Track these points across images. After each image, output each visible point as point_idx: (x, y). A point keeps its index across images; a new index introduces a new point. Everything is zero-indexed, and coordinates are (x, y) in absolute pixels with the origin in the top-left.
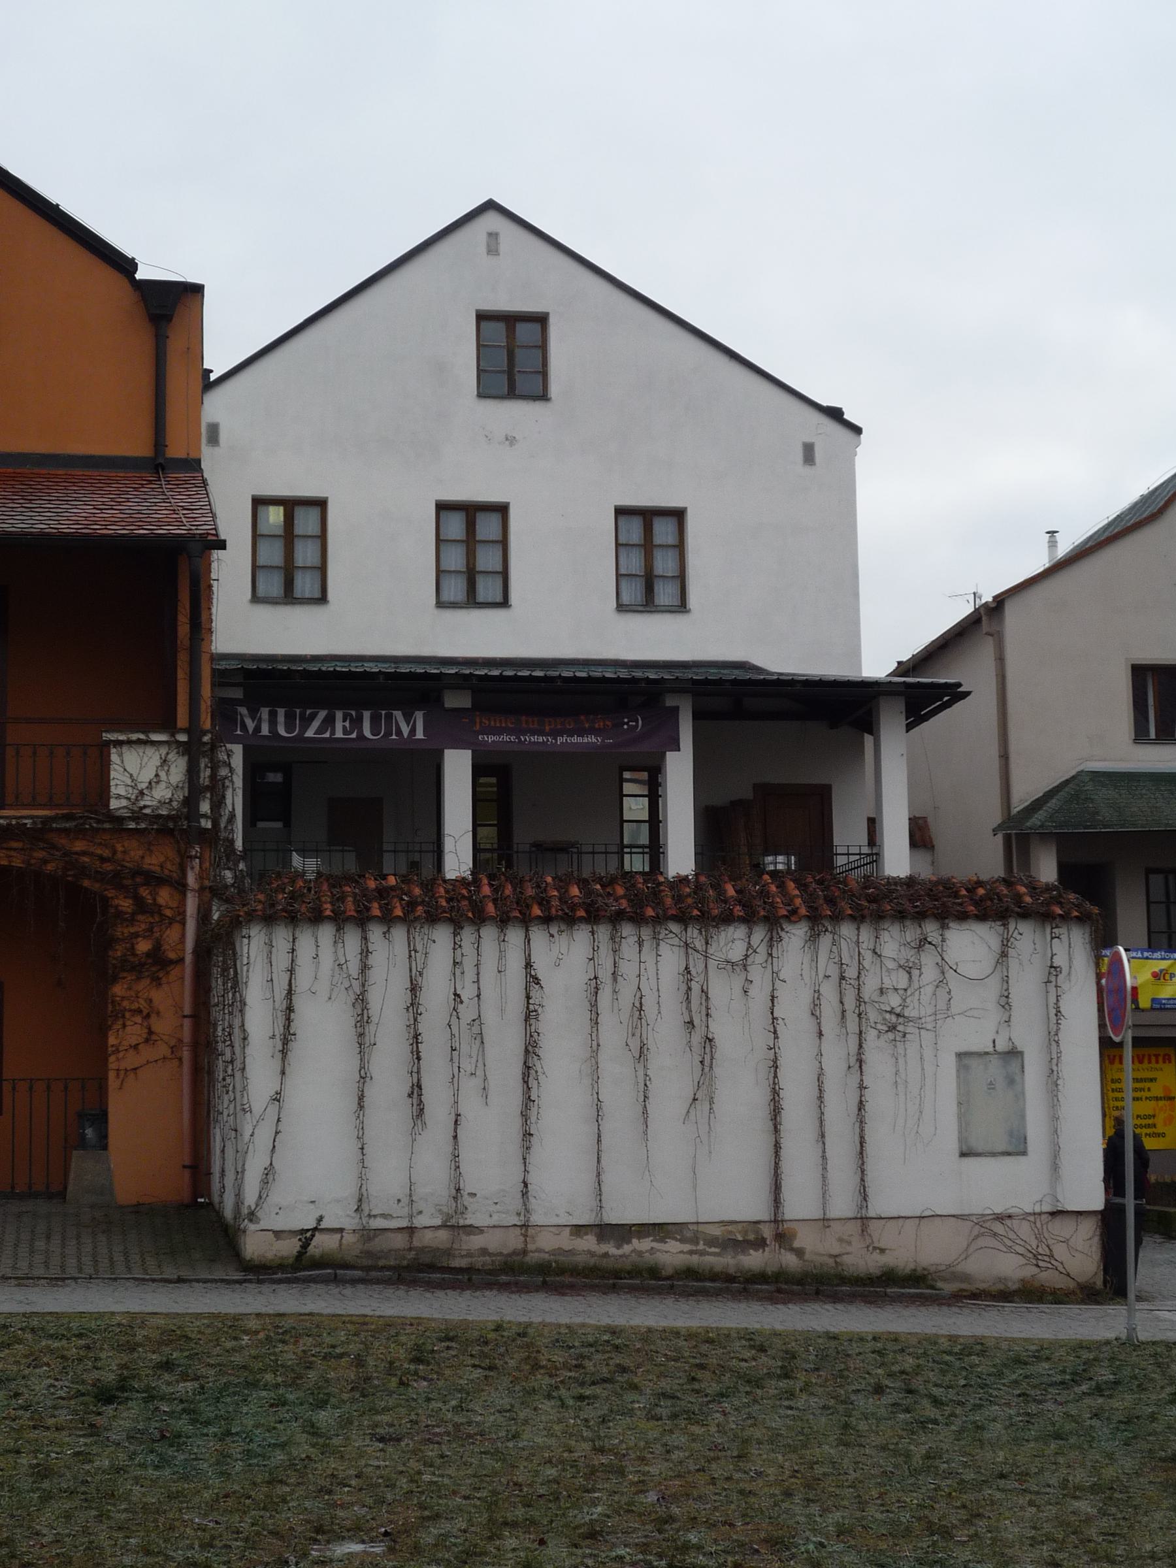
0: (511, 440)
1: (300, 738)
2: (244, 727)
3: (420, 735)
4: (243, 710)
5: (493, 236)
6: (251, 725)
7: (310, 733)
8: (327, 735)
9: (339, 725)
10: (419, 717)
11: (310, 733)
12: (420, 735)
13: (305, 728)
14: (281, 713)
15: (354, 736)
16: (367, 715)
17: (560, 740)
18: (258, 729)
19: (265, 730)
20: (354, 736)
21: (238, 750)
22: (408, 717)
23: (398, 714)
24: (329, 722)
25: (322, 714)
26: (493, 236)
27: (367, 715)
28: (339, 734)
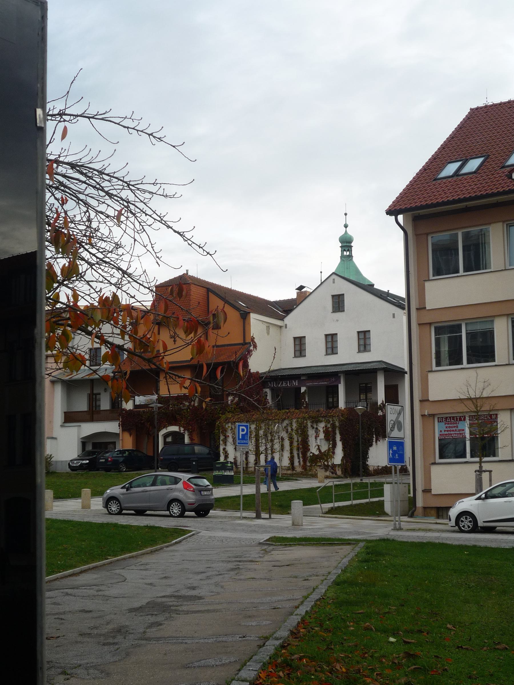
1: (278, 387)
3: (297, 385)
5: (334, 279)
6: (270, 385)
7: (279, 386)
10: (297, 381)
11: (279, 386)
12: (297, 385)
14: (275, 382)
16: (288, 382)
19: (272, 386)
21: (268, 391)
22: (295, 382)
23: (293, 381)
24: (282, 383)
25: (281, 382)
26: (334, 279)
27: (288, 382)
28: (284, 386)
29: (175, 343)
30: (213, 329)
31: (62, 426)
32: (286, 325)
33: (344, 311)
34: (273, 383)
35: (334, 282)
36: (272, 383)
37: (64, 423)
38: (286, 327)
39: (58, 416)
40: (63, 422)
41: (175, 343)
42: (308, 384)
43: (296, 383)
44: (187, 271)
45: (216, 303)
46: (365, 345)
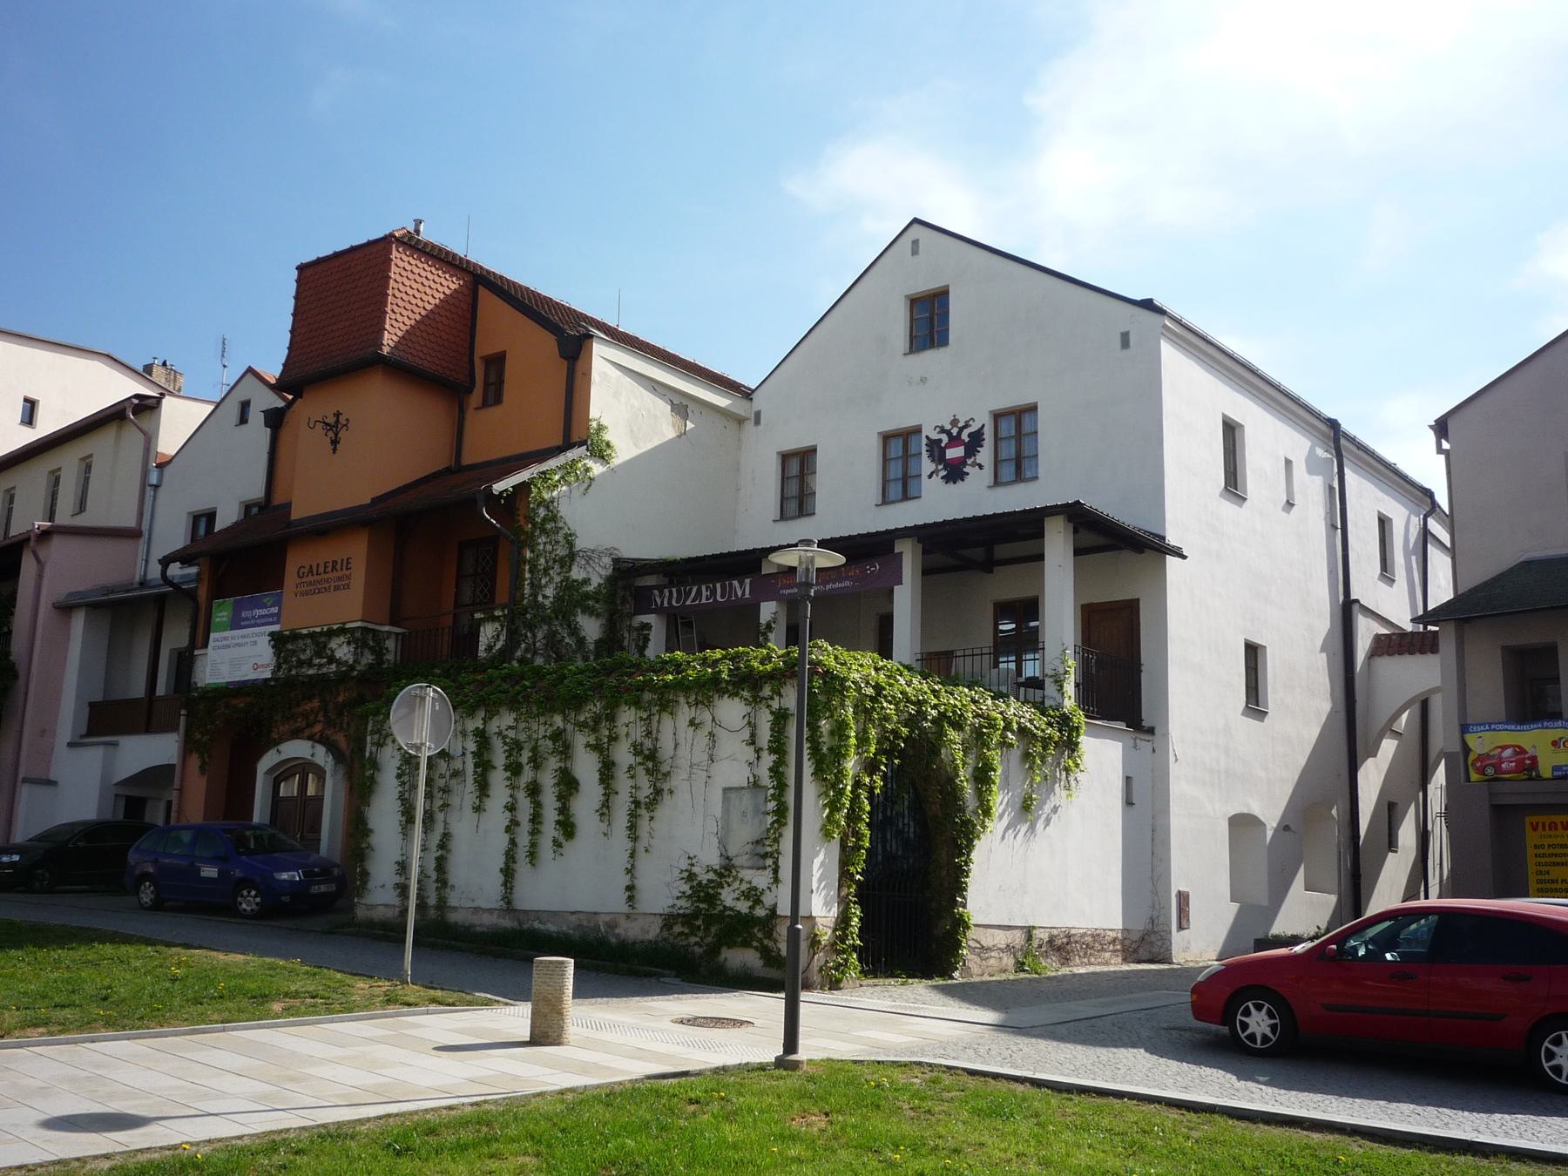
0: (923, 380)
2: (656, 605)
3: (747, 596)
4: (656, 592)
5: (915, 243)
7: (688, 603)
8: (697, 602)
9: (704, 593)
10: (747, 581)
11: (688, 603)
12: (747, 596)
13: (685, 601)
15: (711, 601)
16: (718, 586)
17: (828, 587)
18: (662, 603)
19: (666, 605)
20: (711, 601)
22: (742, 584)
23: (735, 583)
25: (695, 589)
26: (915, 243)
27: (718, 586)
28: (704, 601)
29: (335, 450)
30: (485, 404)
31: (71, 745)
32: (758, 415)
33: (944, 342)
34: (671, 592)
35: (915, 252)
36: (666, 591)
37: (82, 737)
38: (757, 422)
39: (68, 715)
40: (84, 730)
41: (335, 450)
42: (787, 592)
43: (742, 589)
44: (418, 222)
45: (495, 318)
46: (1018, 462)
